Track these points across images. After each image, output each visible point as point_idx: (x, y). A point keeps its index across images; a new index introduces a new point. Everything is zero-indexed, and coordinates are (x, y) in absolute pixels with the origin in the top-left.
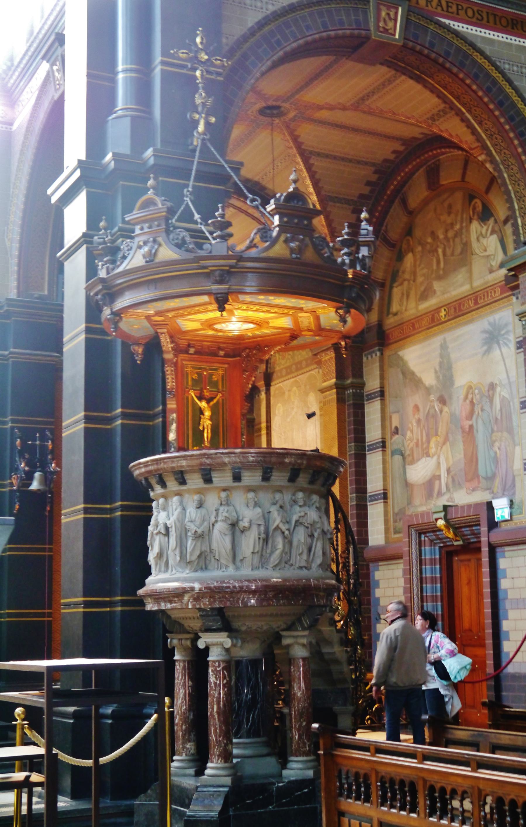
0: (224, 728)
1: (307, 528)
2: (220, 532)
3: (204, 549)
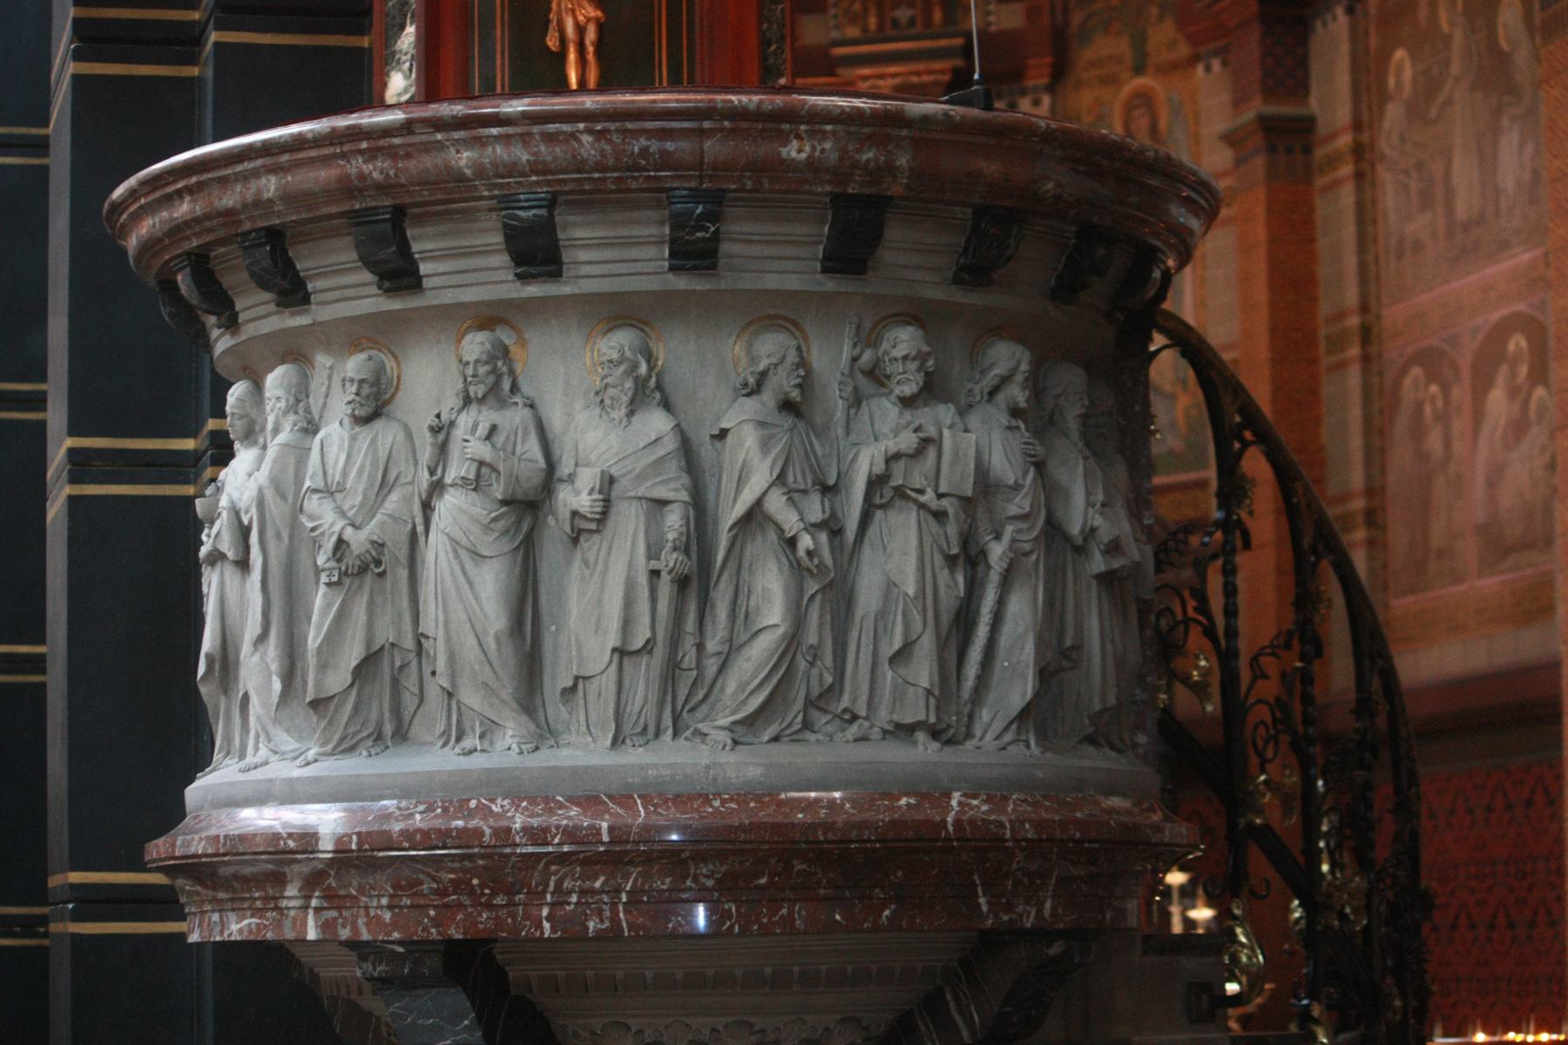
1: (940, 516)
2: (453, 541)
3: (385, 634)
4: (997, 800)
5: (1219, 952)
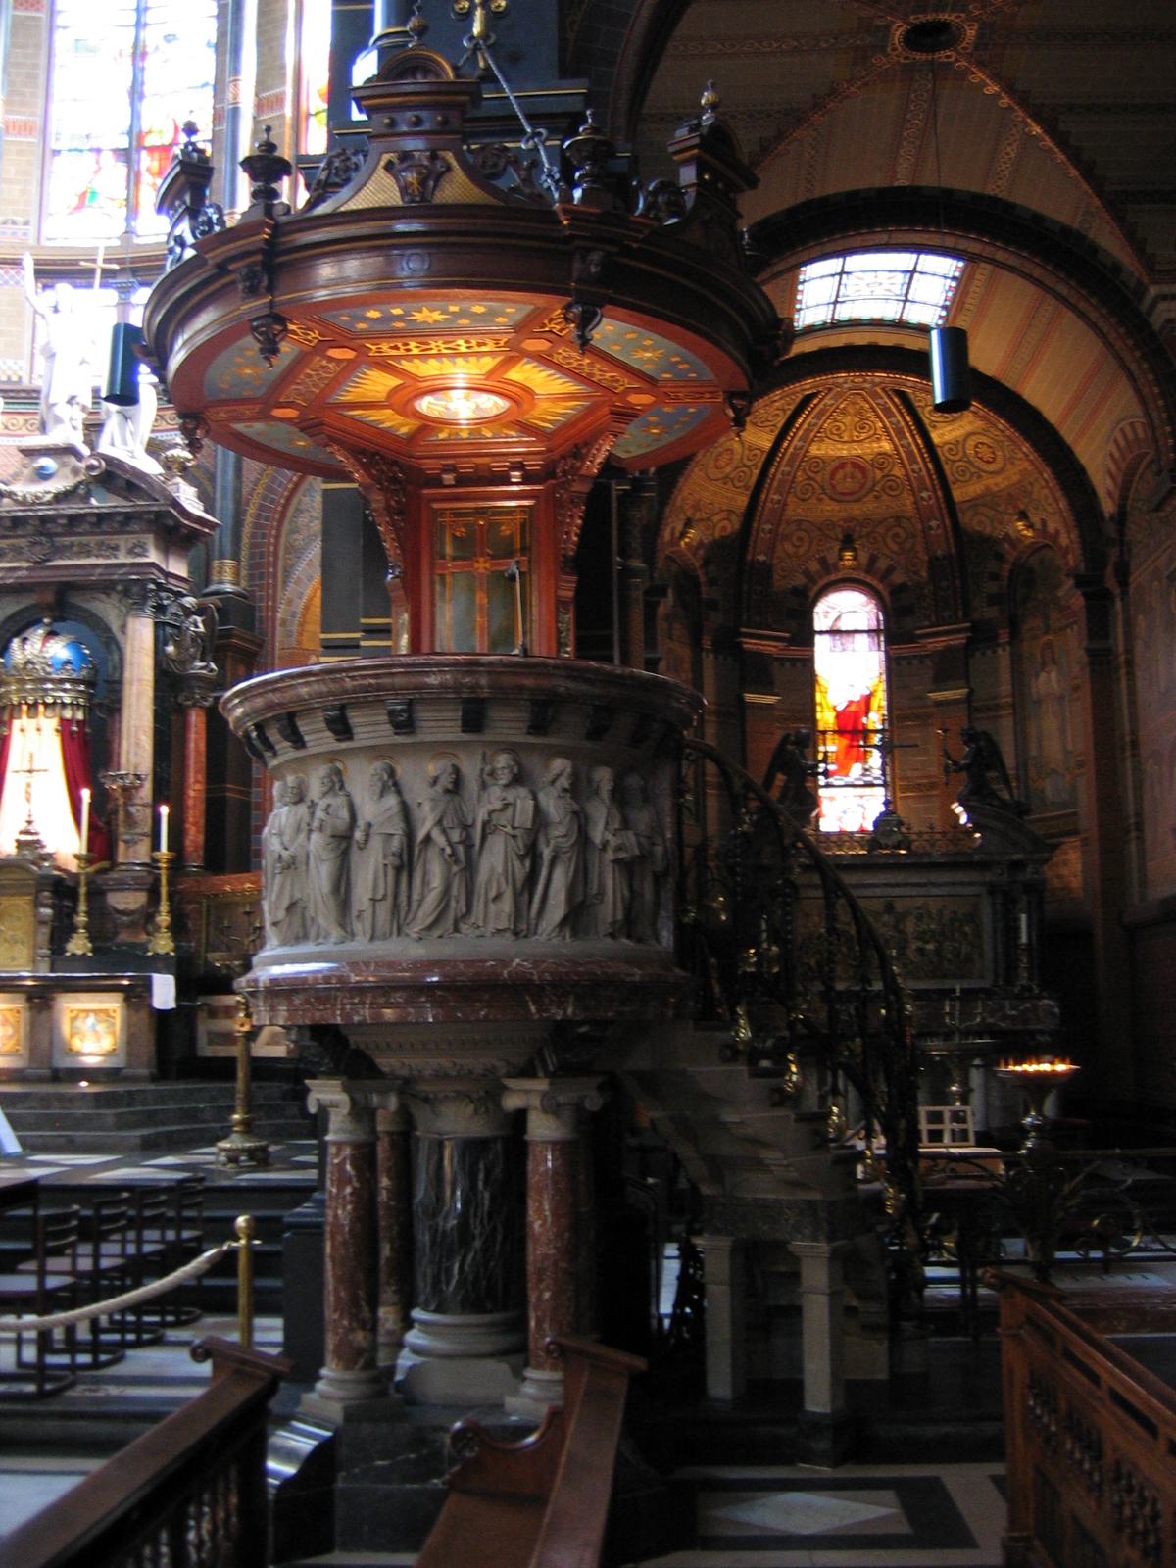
0: (342, 1293)
1: (514, 837)
4: (536, 964)
5: (729, 1030)
